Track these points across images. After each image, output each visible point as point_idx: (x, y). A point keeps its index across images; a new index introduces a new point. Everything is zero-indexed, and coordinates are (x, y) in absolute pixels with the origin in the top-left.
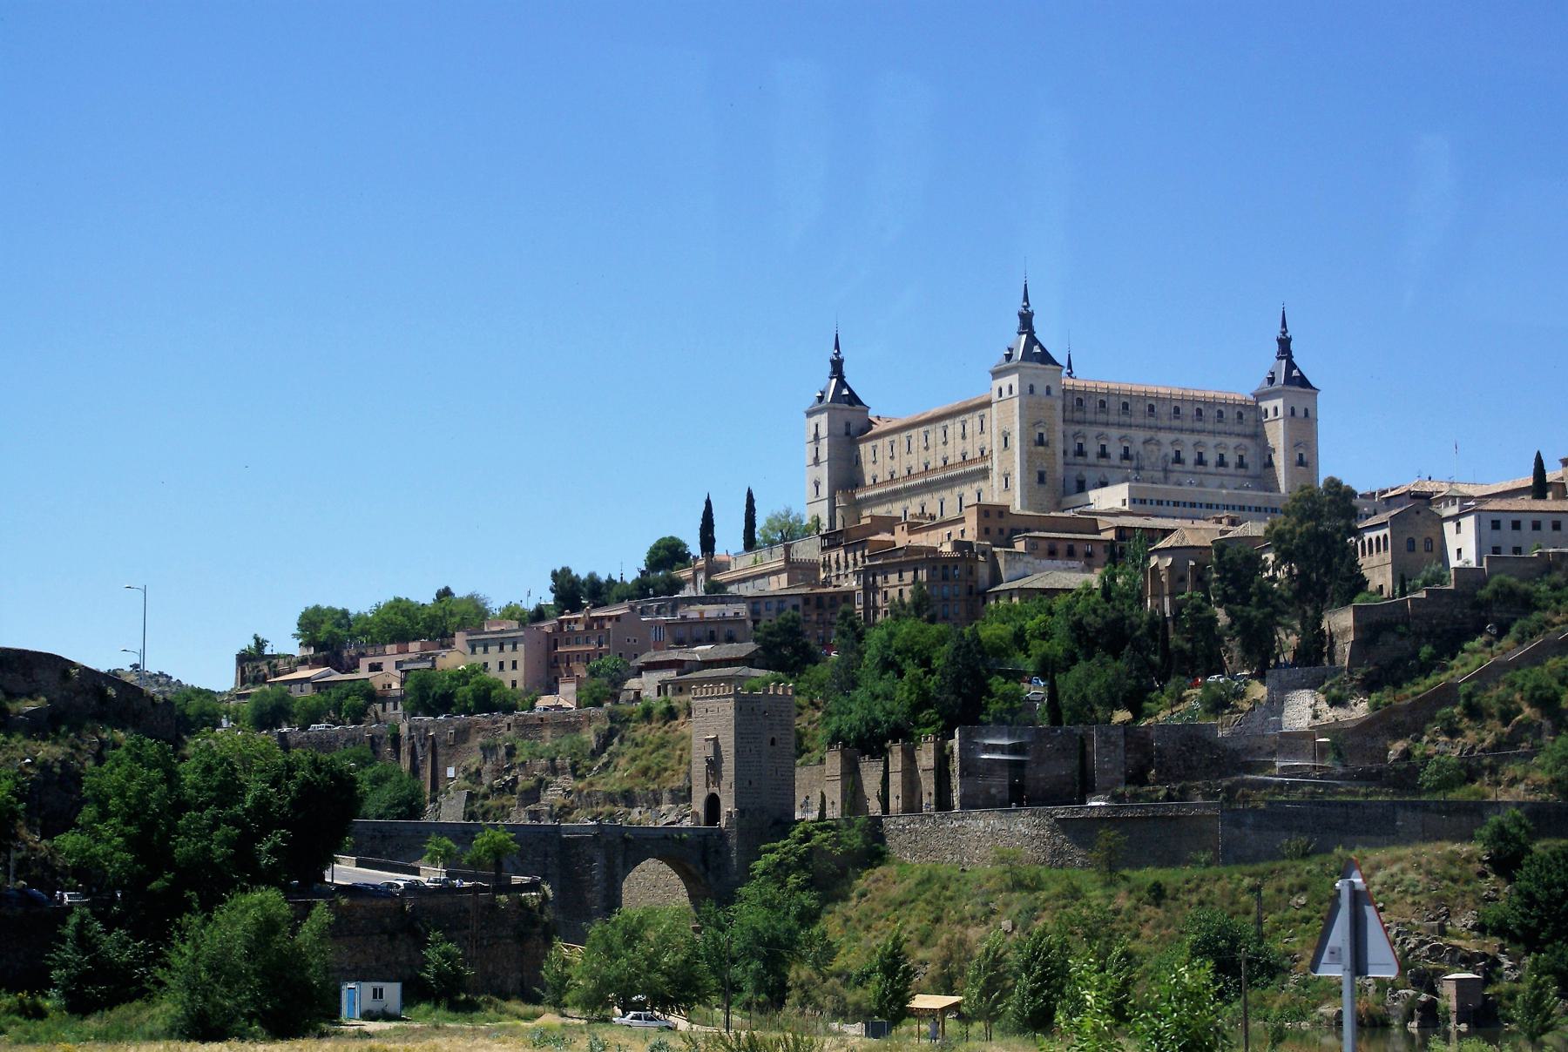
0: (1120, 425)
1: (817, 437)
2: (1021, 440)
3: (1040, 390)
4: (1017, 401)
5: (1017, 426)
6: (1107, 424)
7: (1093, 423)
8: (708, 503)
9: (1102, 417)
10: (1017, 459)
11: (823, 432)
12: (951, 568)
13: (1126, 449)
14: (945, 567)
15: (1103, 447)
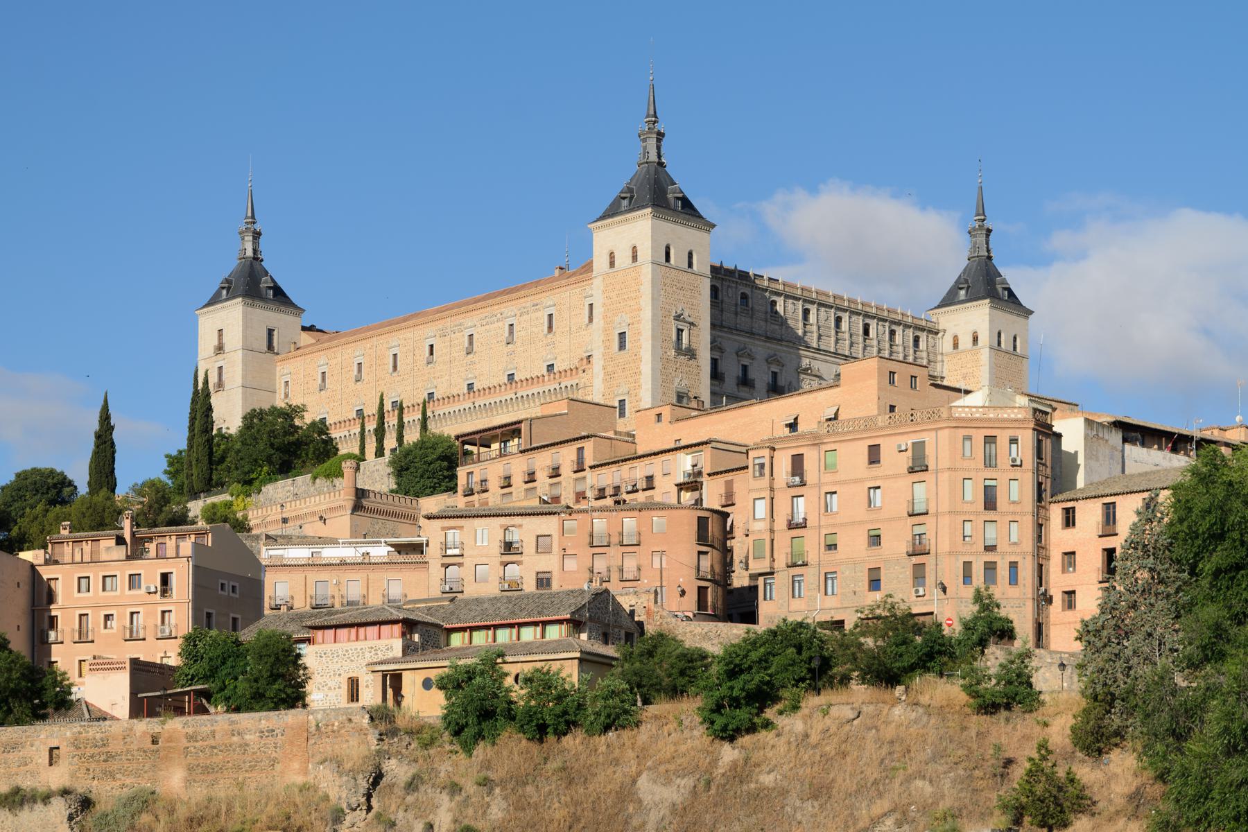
0: (769, 339)
1: (220, 348)
2: (654, 337)
3: (677, 258)
4: (646, 271)
5: (647, 314)
6: (752, 334)
7: (735, 330)
8: (105, 418)
9: (743, 321)
10: (646, 367)
11: (234, 340)
12: (1003, 438)
13: (775, 374)
14: (990, 440)
15: (745, 368)
